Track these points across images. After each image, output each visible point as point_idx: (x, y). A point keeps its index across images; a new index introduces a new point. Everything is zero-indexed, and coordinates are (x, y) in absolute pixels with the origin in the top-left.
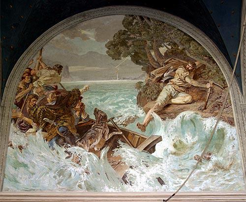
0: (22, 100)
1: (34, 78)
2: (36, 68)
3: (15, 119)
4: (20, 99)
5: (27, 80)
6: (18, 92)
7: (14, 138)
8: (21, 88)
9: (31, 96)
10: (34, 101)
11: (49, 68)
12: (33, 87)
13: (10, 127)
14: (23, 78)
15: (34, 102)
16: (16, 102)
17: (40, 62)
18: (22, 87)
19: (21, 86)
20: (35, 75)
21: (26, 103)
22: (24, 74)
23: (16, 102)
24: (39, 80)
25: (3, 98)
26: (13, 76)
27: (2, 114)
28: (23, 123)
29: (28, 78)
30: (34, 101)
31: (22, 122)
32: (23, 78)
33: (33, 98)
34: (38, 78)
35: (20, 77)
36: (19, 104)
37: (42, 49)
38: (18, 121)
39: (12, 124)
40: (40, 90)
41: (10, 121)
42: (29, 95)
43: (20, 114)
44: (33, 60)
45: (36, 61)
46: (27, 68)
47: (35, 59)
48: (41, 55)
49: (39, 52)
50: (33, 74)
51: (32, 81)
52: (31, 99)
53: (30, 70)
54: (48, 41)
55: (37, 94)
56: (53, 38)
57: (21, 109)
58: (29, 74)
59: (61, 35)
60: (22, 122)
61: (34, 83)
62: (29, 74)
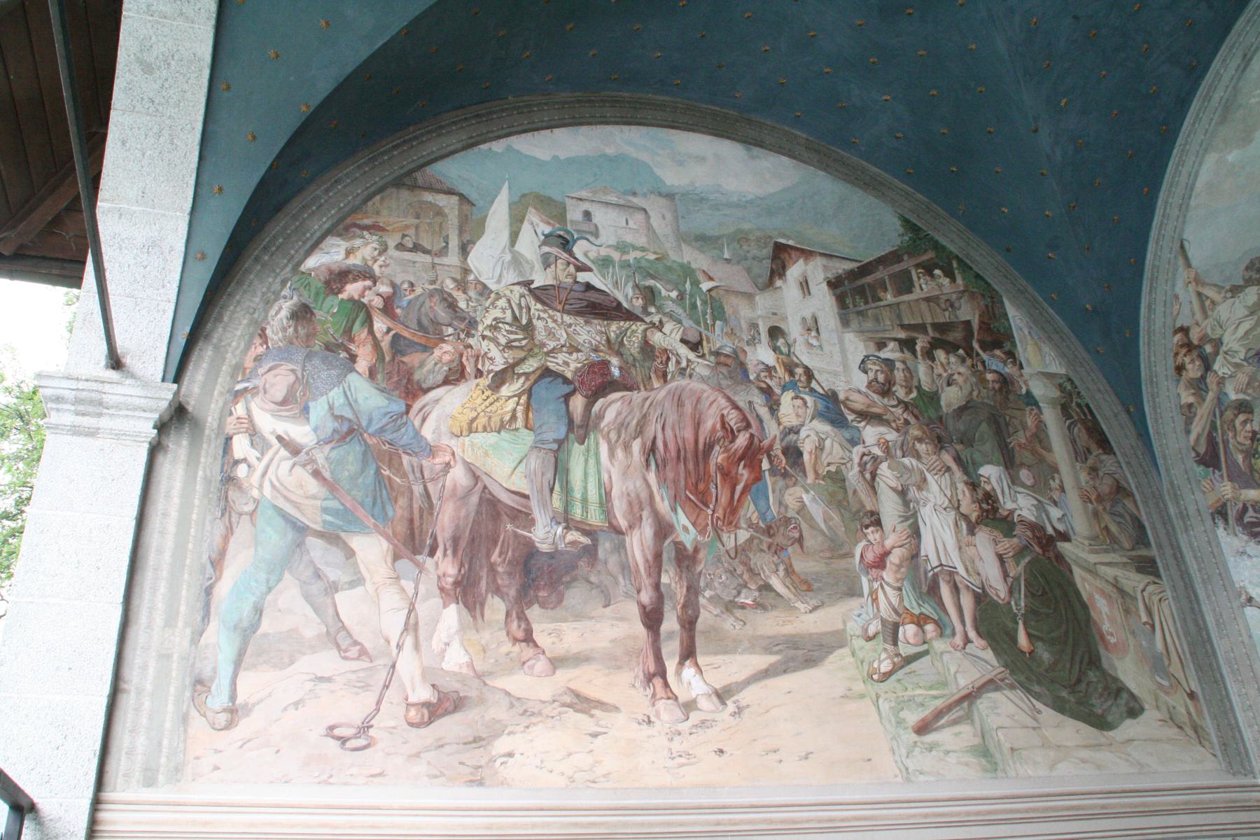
0: (1212, 442)
1: (1208, 349)
2: (1199, 316)
3: (1221, 512)
4: (1203, 440)
5: (1193, 370)
6: (1189, 422)
7: (1247, 574)
8: (1190, 406)
9: (1229, 414)
10: (1245, 422)
11: (1235, 290)
12: (1221, 382)
13: (1218, 545)
14: (1180, 369)
15: (1248, 427)
16: (1198, 454)
17: (1200, 289)
18: (1191, 400)
19: (1187, 397)
20: (1205, 339)
21: (1226, 443)
22: (1177, 354)
23: (1198, 454)
24: (1224, 348)
25: (1160, 462)
26: (1152, 382)
27: (1181, 513)
28: (1251, 512)
29: (1192, 361)
30: (1245, 422)
31: (1245, 509)
32: (1180, 369)
33: (1236, 416)
34: (1218, 343)
35: (1172, 372)
36: (1210, 458)
37: (1182, 247)
38: (1232, 513)
39: (1221, 532)
40: (1242, 378)
41: (1209, 522)
42: (1222, 414)
43: (1226, 489)
44: (1177, 297)
45: (1186, 295)
46: (1176, 332)
47: (1179, 289)
48: (1188, 264)
49: (1181, 261)
50: (1201, 339)
51: (1207, 365)
52: (1233, 421)
53: (1184, 330)
54: (1184, 207)
55: (1241, 396)
56: (1192, 189)
57: (1220, 470)
58: (1189, 346)
59: (1210, 160)
60: (1245, 509)
61: (1216, 367)
62: (1189, 346)
